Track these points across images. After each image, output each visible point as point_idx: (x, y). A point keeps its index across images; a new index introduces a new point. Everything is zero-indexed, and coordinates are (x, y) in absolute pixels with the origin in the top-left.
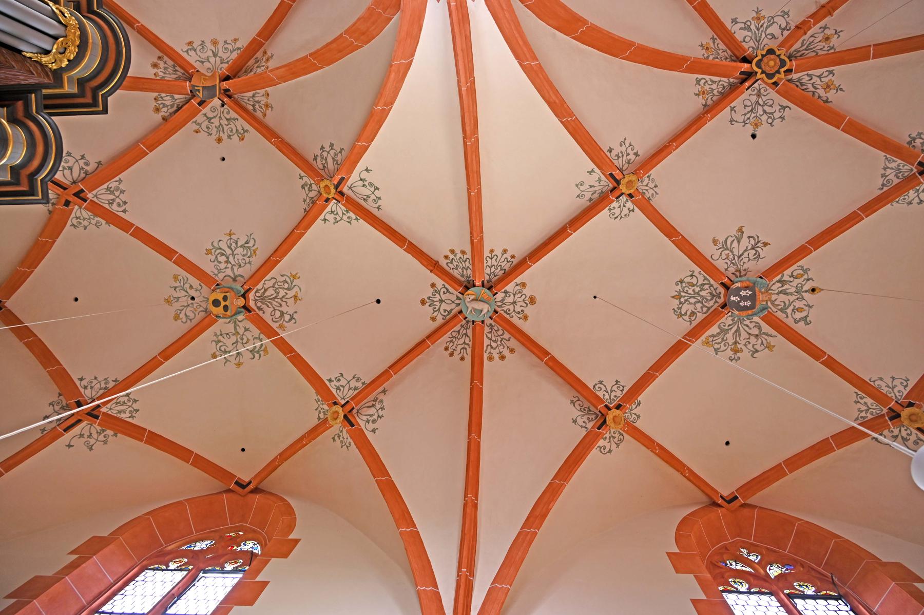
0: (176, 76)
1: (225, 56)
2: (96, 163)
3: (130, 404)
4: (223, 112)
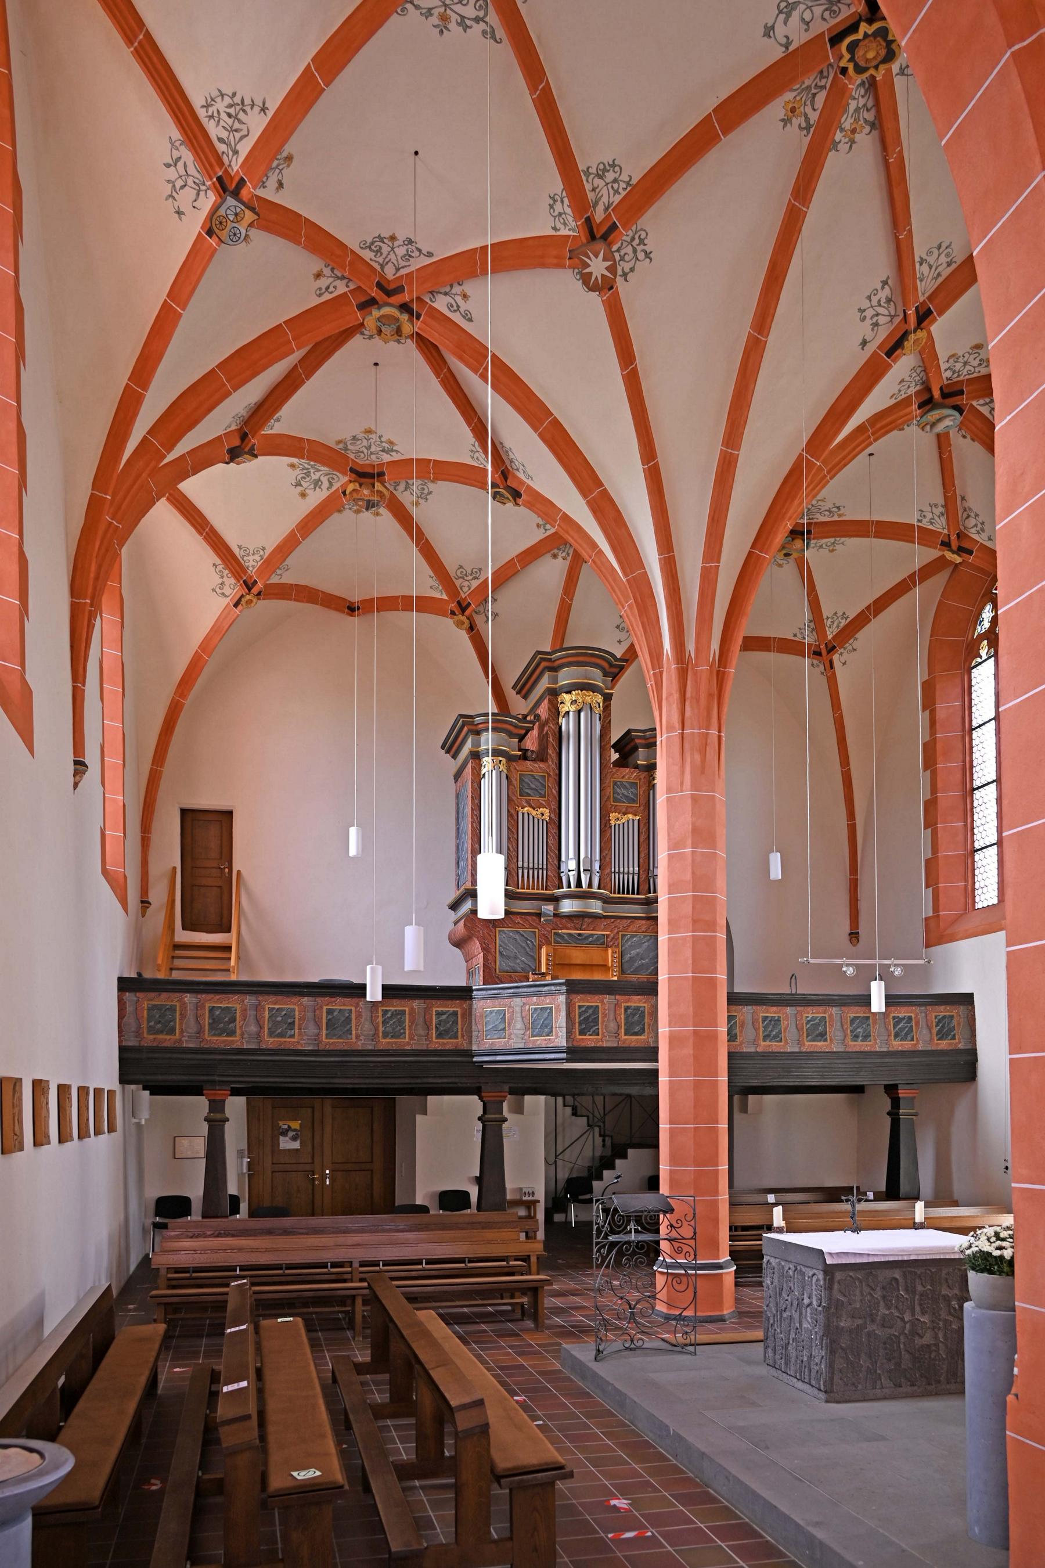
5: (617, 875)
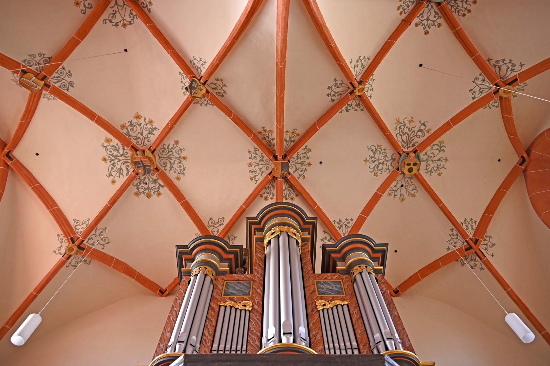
0: (272, 187)
1: (259, 159)
3: (467, 223)
4: (292, 161)
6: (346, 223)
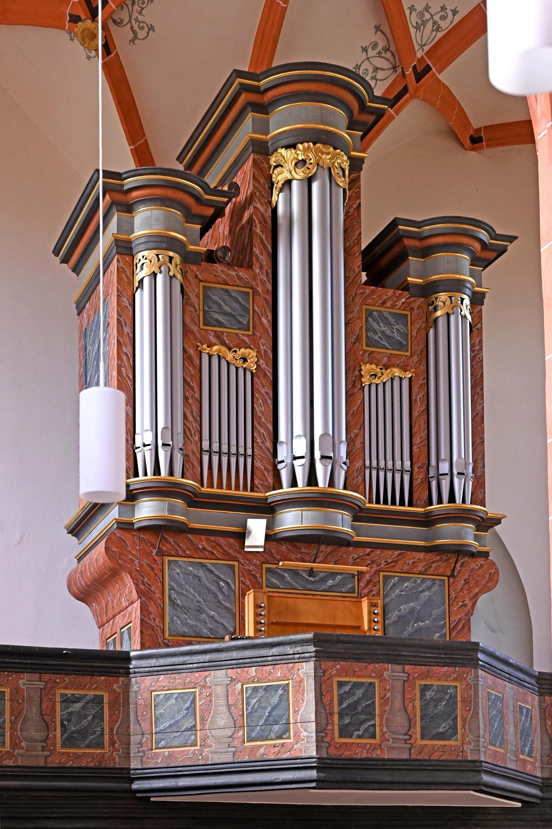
2: (376, 34)
5: (374, 473)
6: (437, 18)
